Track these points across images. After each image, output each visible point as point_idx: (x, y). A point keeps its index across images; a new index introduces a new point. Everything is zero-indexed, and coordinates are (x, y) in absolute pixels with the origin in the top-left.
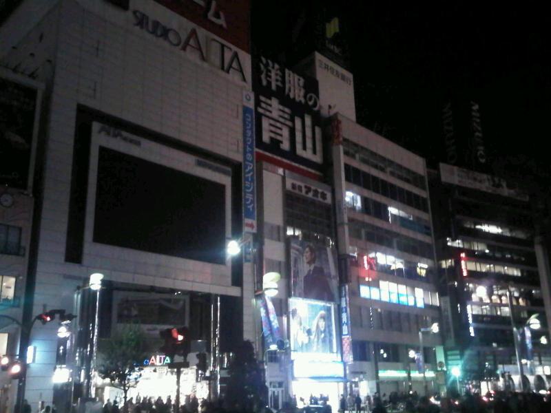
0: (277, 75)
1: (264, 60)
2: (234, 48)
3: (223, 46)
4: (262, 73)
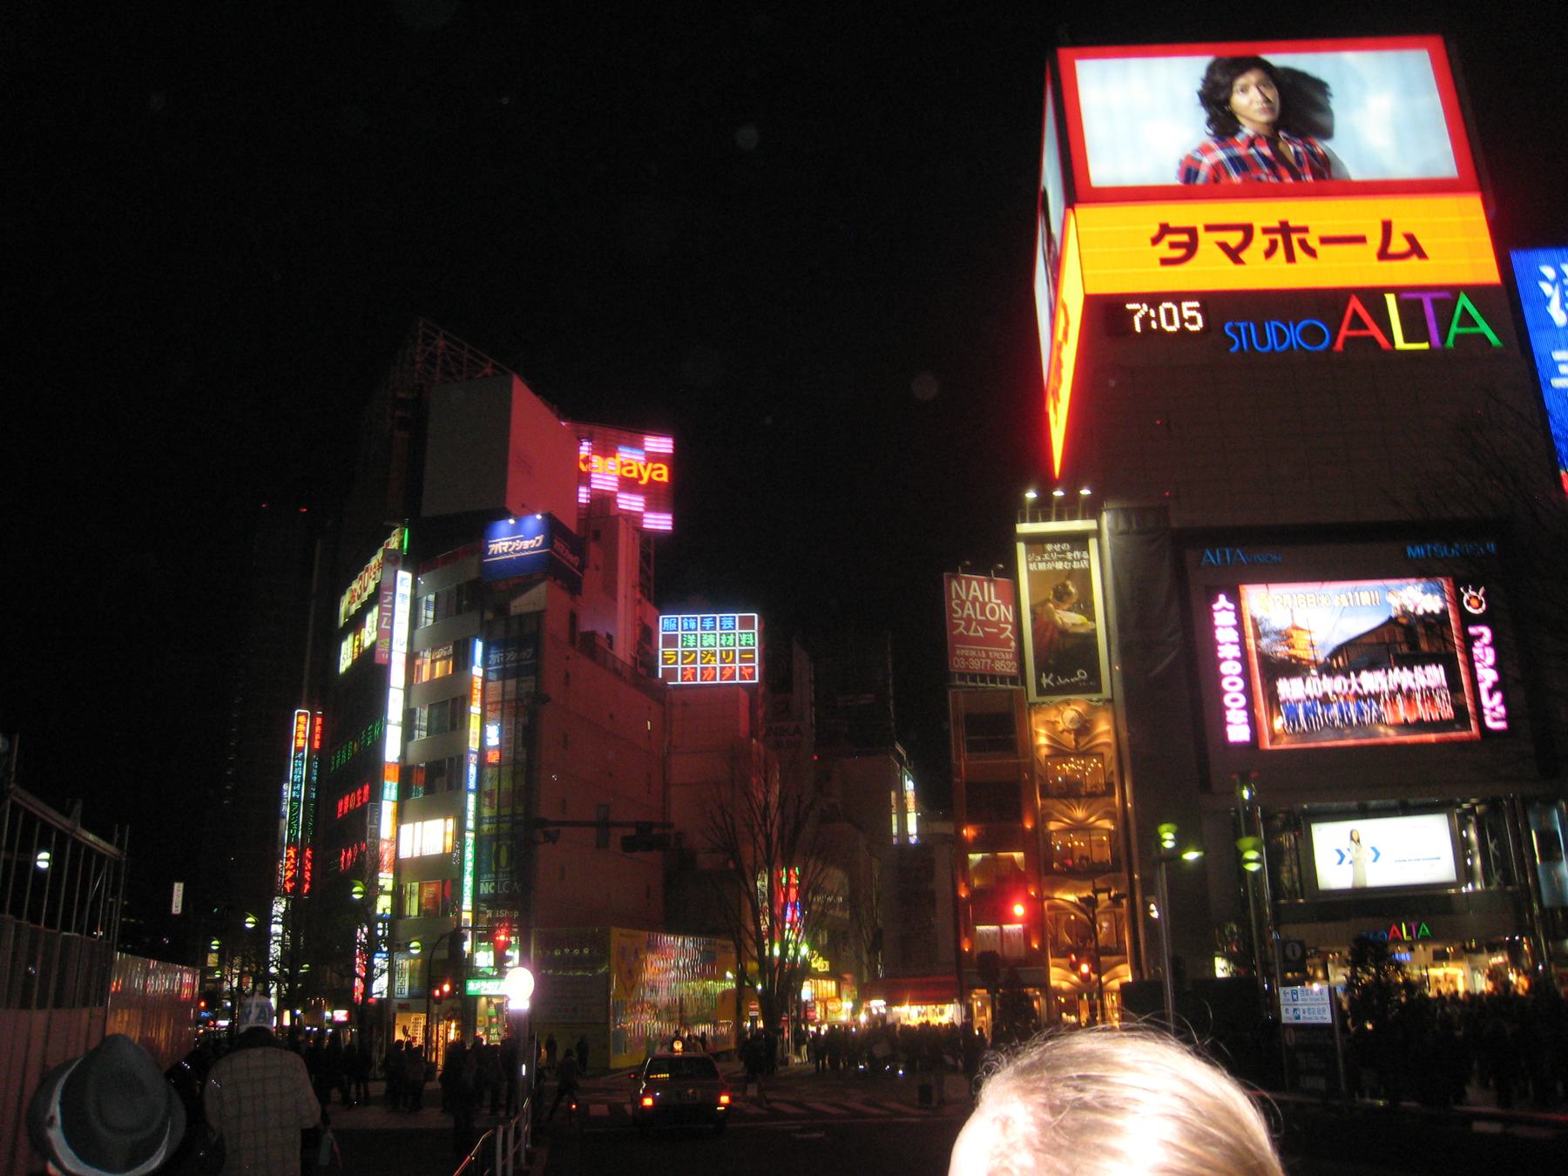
1: (1549, 272)
4: (1547, 300)
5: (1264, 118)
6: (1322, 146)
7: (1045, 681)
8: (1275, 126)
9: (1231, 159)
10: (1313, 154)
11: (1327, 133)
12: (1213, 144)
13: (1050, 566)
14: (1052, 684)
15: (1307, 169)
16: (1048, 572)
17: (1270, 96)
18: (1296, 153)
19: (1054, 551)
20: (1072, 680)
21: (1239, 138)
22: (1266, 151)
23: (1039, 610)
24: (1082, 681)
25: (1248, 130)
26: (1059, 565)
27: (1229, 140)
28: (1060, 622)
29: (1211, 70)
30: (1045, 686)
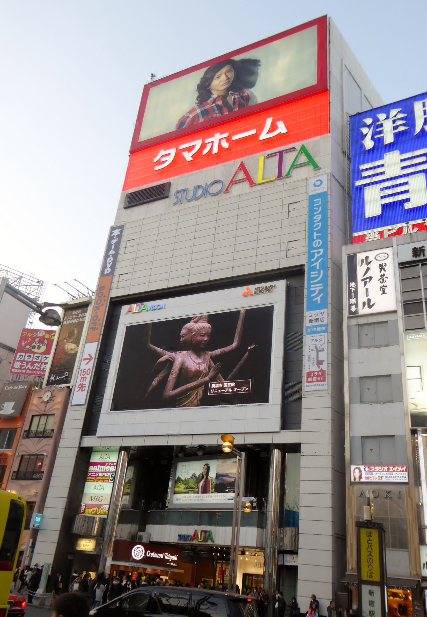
0: (394, 122)
1: (369, 121)
2: (298, 145)
3: (281, 154)
5: (224, 88)
6: (247, 92)
7: (52, 378)
8: (228, 90)
9: (202, 112)
10: (242, 97)
11: (252, 85)
12: (196, 107)
13: (71, 322)
14: (54, 380)
15: (237, 105)
16: (70, 324)
17: (229, 76)
18: (234, 99)
19: (75, 314)
20: (62, 377)
21: (208, 102)
22: (220, 103)
23: (60, 344)
24: (65, 377)
25: (214, 96)
26: (75, 321)
27: (204, 103)
28: (66, 349)
29: (206, 73)
30: (51, 381)
